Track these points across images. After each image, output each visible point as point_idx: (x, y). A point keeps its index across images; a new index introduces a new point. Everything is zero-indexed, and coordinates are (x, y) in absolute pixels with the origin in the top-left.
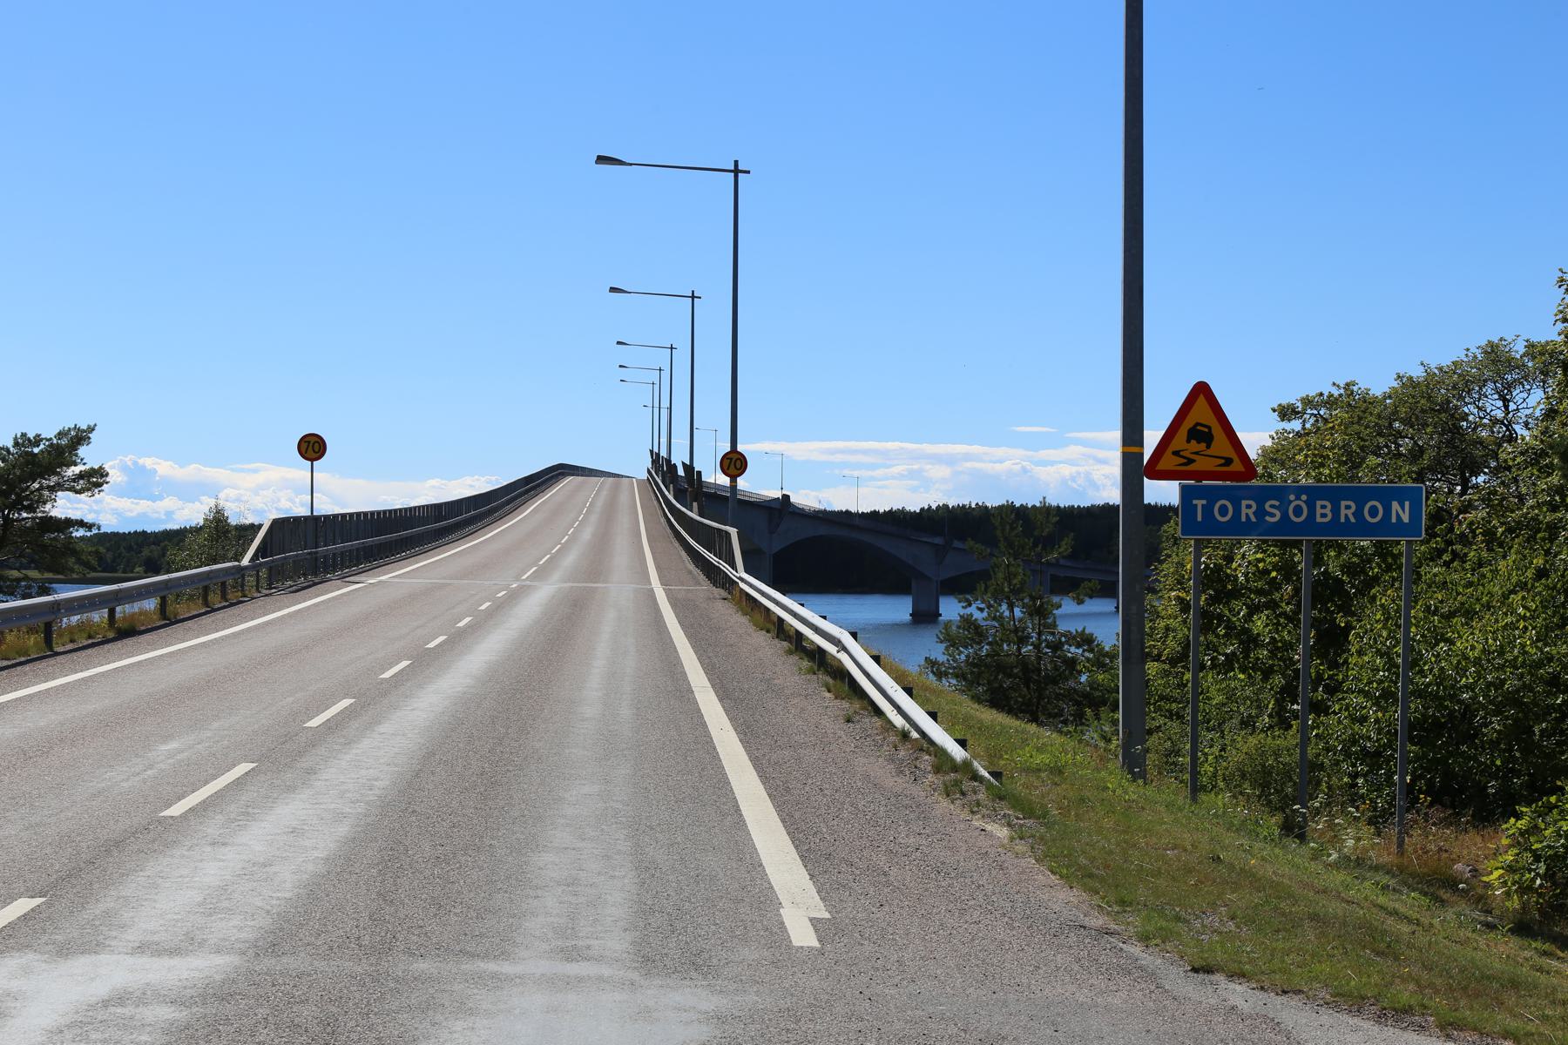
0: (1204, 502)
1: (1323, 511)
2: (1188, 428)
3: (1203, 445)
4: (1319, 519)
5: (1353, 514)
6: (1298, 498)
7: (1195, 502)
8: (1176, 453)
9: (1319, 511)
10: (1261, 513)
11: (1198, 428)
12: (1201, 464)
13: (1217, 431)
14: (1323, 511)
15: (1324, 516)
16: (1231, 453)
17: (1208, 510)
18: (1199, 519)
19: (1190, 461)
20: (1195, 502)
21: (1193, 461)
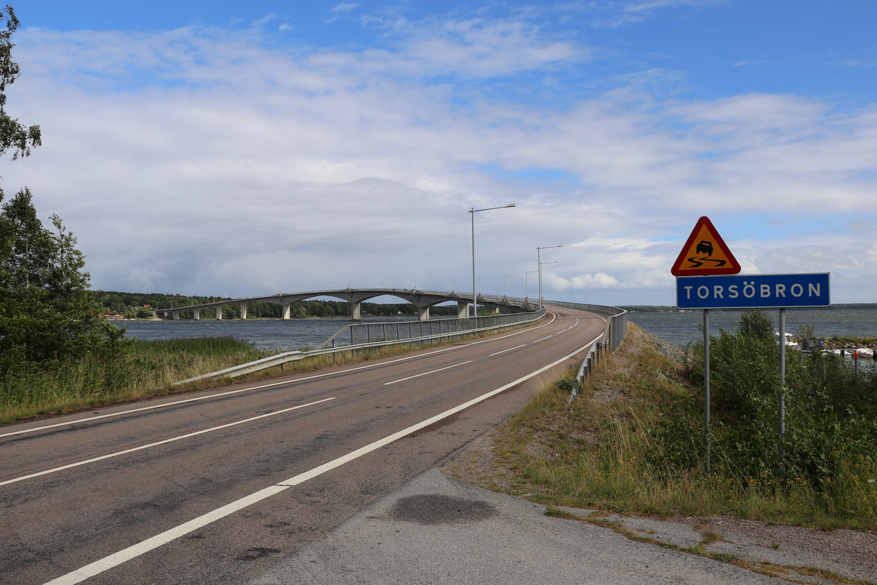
0: (691, 287)
1: (765, 291)
2: (697, 245)
3: (707, 254)
4: (762, 296)
5: (784, 292)
6: (749, 283)
7: (685, 287)
8: (691, 260)
9: (762, 291)
10: (726, 293)
11: (704, 244)
12: (706, 265)
13: (715, 245)
14: (765, 291)
15: (765, 293)
16: (724, 258)
17: (693, 292)
18: (689, 297)
19: (699, 264)
20: (685, 287)
21: (702, 264)
